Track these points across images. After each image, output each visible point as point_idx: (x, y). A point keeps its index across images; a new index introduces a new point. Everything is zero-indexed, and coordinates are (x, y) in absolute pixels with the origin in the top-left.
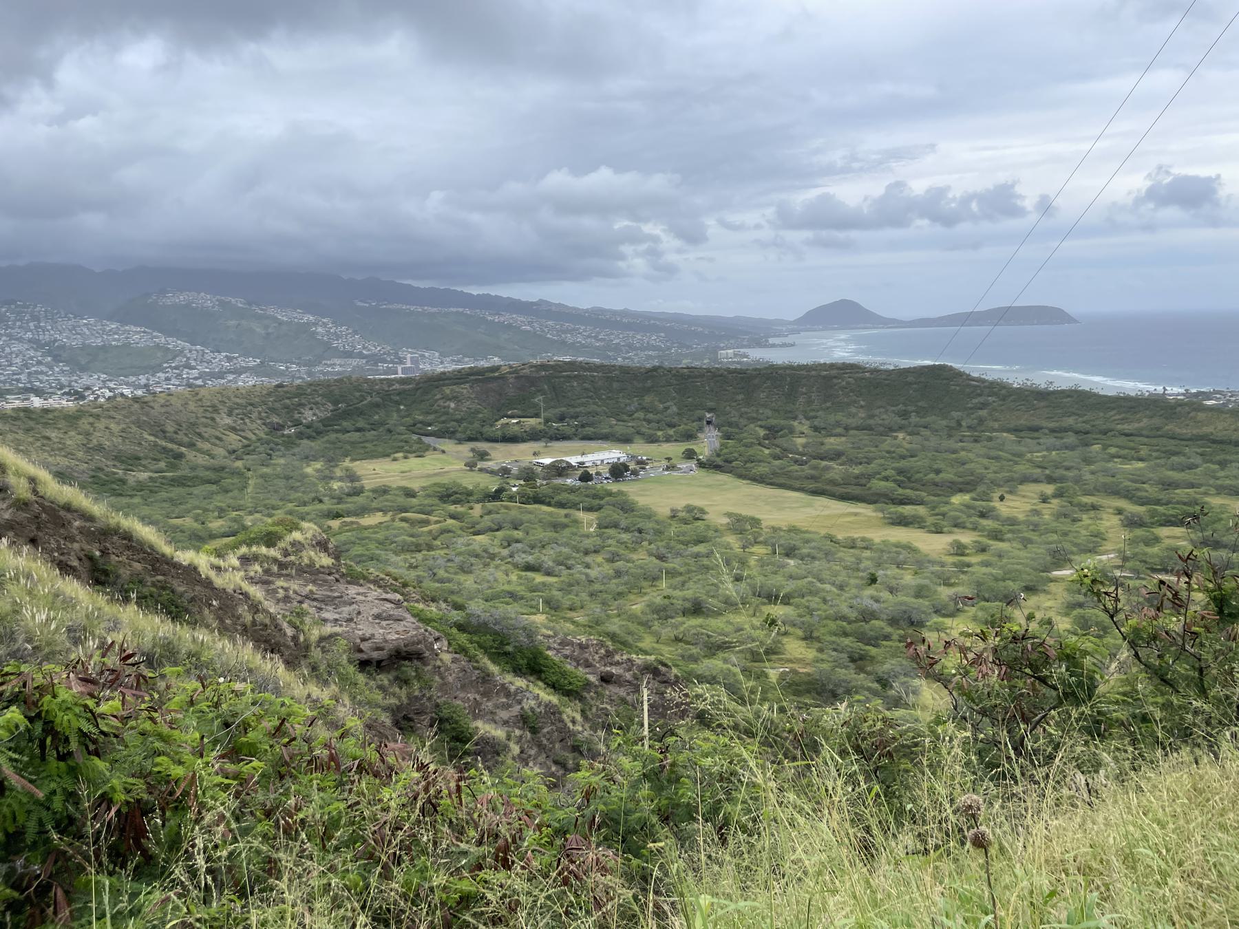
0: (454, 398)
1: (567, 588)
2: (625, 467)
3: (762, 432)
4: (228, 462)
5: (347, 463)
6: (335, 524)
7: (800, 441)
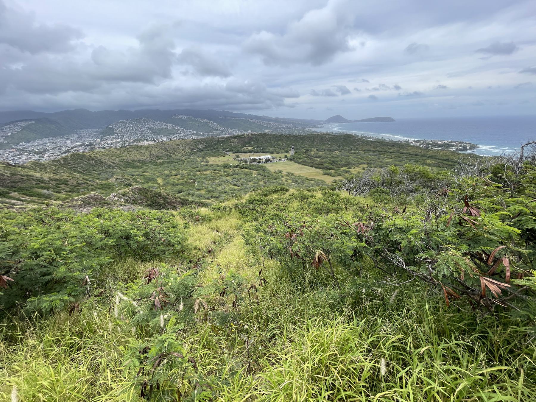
2: (269, 160)
3: (304, 151)
4: (180, 158)
5: (207, 158)
6: (198, 173)
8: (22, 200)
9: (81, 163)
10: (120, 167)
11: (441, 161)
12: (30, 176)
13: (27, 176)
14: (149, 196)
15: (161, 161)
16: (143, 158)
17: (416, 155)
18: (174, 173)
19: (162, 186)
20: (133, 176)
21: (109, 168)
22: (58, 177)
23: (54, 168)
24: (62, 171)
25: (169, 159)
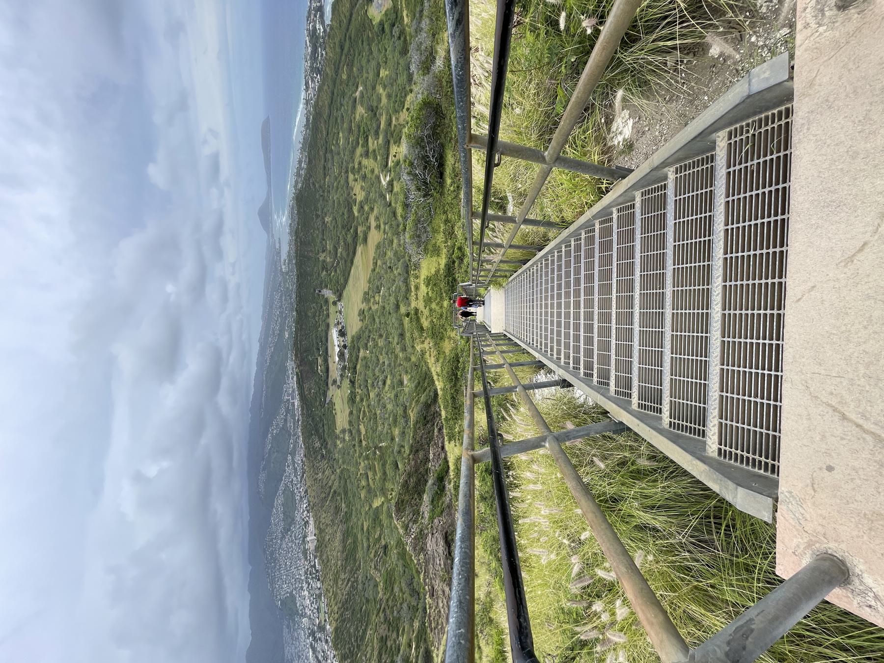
0: (310, 389)
1: (394, 376)
2: (340, 331)
3: (324, 273)
5: (338, 431)
6: (364, 443)
7: (328, 259)
10: (353, 572)
11: (343, 57)
14: (407, 498)
16: (339, 536)
17: (333, 93)
18: (363, 483)
19: (386, 497)
20: (369, 546)
22: (376, 653)
24: (364, 658)
25: (339, 494)
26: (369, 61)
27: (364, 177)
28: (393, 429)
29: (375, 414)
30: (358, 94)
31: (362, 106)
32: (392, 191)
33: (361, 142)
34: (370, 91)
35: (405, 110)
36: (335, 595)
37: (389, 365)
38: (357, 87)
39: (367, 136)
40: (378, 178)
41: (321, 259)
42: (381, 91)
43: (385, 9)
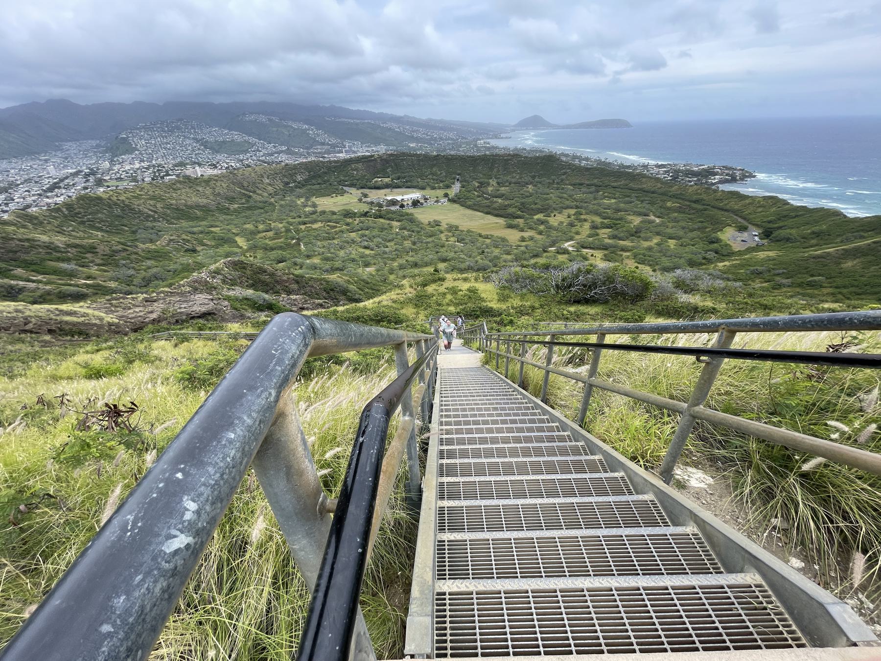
1: (374, 257)
2: (418, 201)
3: (477, 184)
5: (314, 199)
6: (303, 227)
8: (33, 281)
9: (98, 212)
10: (165, 217)
11: (688, 203)
12: (34, 240)
13: (28, 240)
14: (248, 272)
15: (236, 206)
16: (203, 201)
17: (653, 193)
18: (261, 227)
19: (247, 251)
20: (194, 233)
21: (148, 221)
22: (77, 241)
23: (56, 223)
24: (71, 228)
25: (248, 201)
26: (683, 228)
27: (572, 225)
28: (320, 257)
29: (334, 239)
30: (652, 217)
31: (641, 222)
32: (558, 253)
33: (606, 221)
34: (655, 230)
35: (636, 264)
36: (138, 197)
37: (385, 253)
38: (659, 217)
39: (611, 227)
40: (571, 239)
41: (491, 181)
42: (655, 241)
43: (732, 244)
